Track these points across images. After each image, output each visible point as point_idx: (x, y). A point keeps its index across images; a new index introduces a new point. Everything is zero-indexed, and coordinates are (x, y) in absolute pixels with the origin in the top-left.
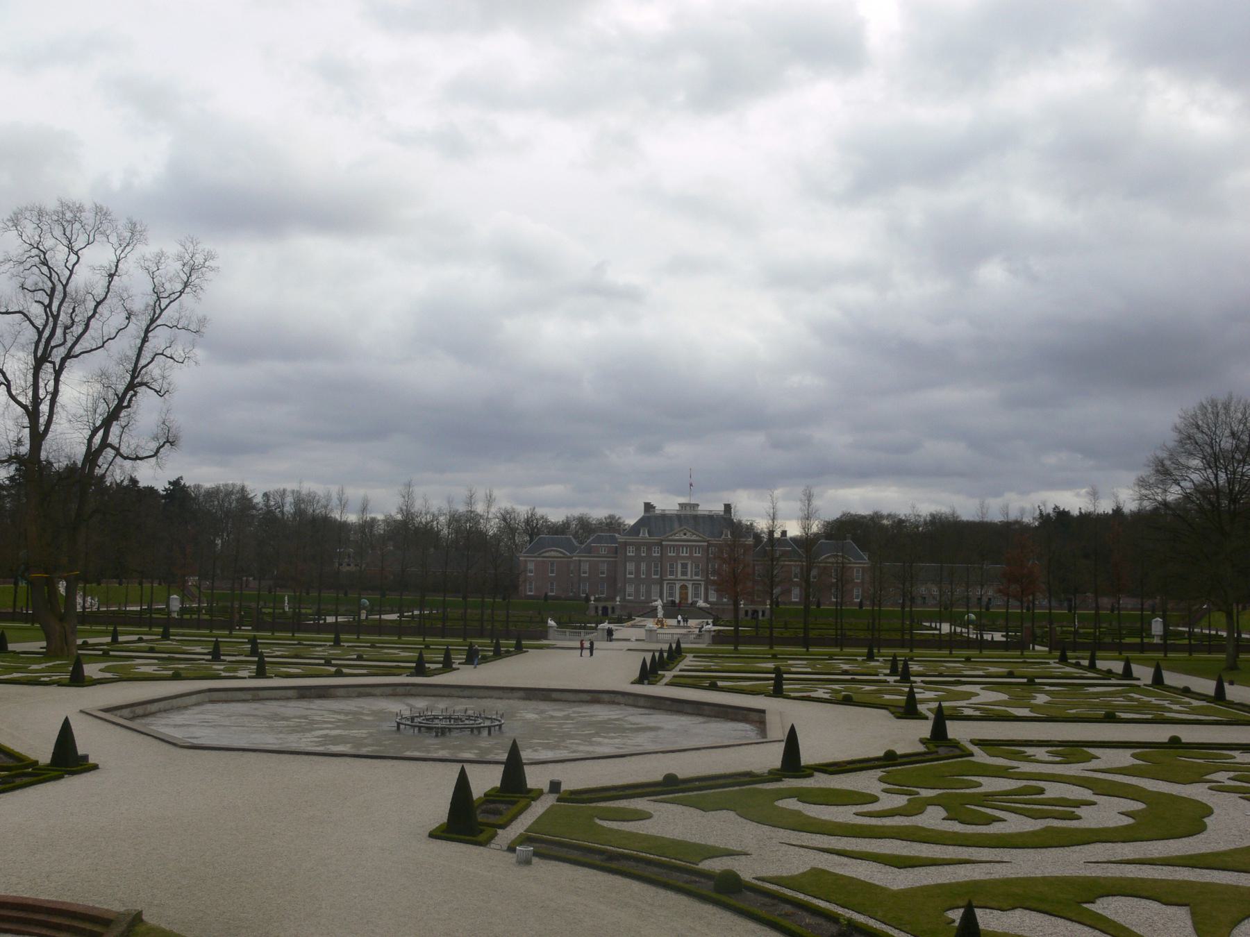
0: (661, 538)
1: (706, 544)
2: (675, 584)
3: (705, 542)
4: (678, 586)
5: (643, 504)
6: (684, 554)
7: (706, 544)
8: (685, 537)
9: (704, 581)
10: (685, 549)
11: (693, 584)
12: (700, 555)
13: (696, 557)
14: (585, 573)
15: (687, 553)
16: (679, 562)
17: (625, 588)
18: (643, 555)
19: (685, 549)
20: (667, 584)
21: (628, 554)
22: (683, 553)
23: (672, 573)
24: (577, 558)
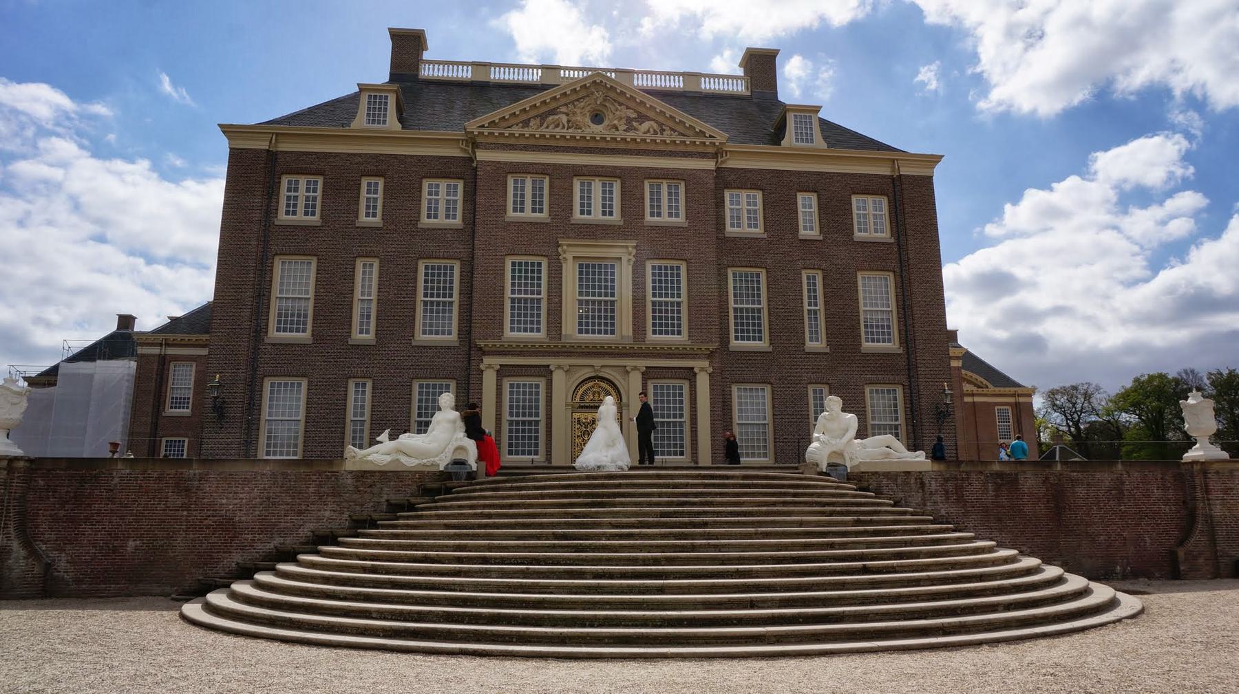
0: (472, 126)
1: (710, 165)
2: (546, 372)
3: (703, 155)
5: (387, 45)
6: (597, 216)
7: (710, 165)
8: (597, 130)
9: (710, 355)
11: (648, 374)
12: (681, 220)
13: (654, 228)
14: (177, 403)
17: (253, 405)
18: (363, 219)
20: (503, 372)
21: (283, 217)
22: (586, 209)
23: (525, 316)
24: (156, 351)
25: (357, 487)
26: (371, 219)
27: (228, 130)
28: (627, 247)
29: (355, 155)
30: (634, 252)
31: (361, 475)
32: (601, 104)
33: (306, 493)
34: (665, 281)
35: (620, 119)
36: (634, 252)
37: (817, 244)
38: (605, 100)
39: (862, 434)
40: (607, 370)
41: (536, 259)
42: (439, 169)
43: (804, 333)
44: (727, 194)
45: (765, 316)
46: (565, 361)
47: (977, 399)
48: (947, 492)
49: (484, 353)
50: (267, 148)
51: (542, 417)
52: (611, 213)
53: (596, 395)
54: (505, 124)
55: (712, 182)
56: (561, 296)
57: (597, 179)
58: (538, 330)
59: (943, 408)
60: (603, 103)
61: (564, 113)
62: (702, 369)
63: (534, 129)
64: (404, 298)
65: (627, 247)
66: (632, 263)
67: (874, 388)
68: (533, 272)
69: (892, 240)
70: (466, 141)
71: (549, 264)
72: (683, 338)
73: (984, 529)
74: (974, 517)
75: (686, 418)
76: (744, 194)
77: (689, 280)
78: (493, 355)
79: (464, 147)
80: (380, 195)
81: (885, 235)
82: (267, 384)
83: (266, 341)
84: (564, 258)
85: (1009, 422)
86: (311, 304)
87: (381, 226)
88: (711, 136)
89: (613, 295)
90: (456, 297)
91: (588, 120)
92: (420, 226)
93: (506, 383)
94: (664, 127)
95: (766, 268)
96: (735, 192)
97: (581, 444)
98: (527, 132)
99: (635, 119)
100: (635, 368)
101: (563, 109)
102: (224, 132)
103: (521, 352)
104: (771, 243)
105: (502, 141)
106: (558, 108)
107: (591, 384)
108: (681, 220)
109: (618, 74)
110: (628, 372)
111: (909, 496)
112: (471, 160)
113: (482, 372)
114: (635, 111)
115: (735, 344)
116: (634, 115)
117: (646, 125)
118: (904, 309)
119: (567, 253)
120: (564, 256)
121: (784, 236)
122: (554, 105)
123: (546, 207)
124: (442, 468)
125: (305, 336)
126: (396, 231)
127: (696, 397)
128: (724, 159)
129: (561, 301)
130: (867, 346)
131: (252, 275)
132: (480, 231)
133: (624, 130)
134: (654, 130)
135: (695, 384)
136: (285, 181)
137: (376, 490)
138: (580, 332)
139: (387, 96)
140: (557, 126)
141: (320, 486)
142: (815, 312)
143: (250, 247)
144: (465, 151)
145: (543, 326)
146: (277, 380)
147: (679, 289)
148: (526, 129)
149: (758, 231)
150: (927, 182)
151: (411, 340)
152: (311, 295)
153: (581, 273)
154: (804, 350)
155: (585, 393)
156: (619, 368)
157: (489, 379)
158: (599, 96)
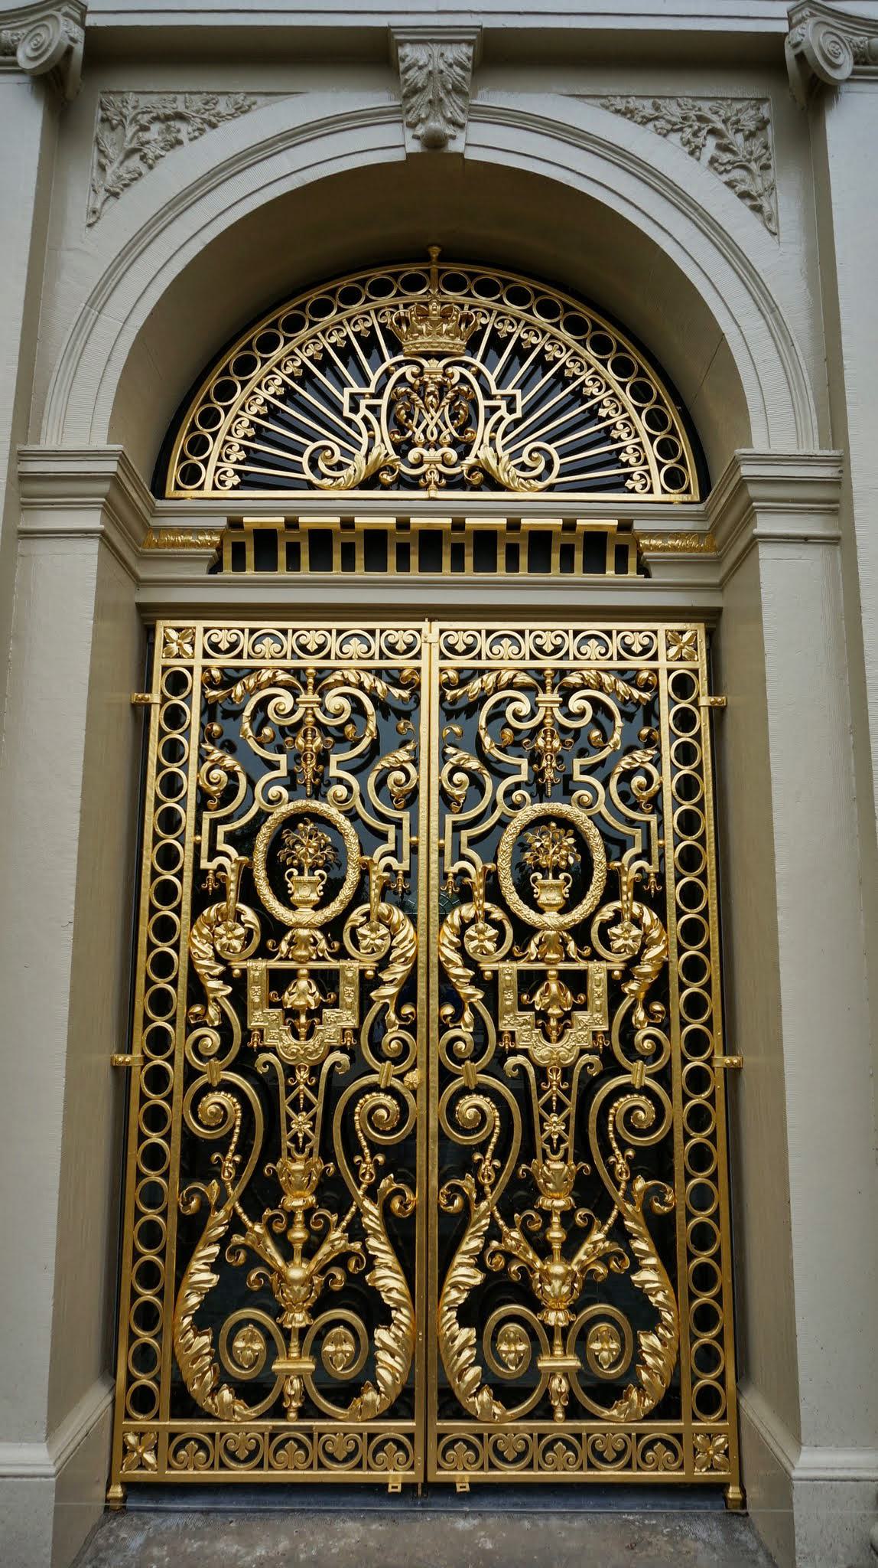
53: (433, 420)
97: (239, 985)
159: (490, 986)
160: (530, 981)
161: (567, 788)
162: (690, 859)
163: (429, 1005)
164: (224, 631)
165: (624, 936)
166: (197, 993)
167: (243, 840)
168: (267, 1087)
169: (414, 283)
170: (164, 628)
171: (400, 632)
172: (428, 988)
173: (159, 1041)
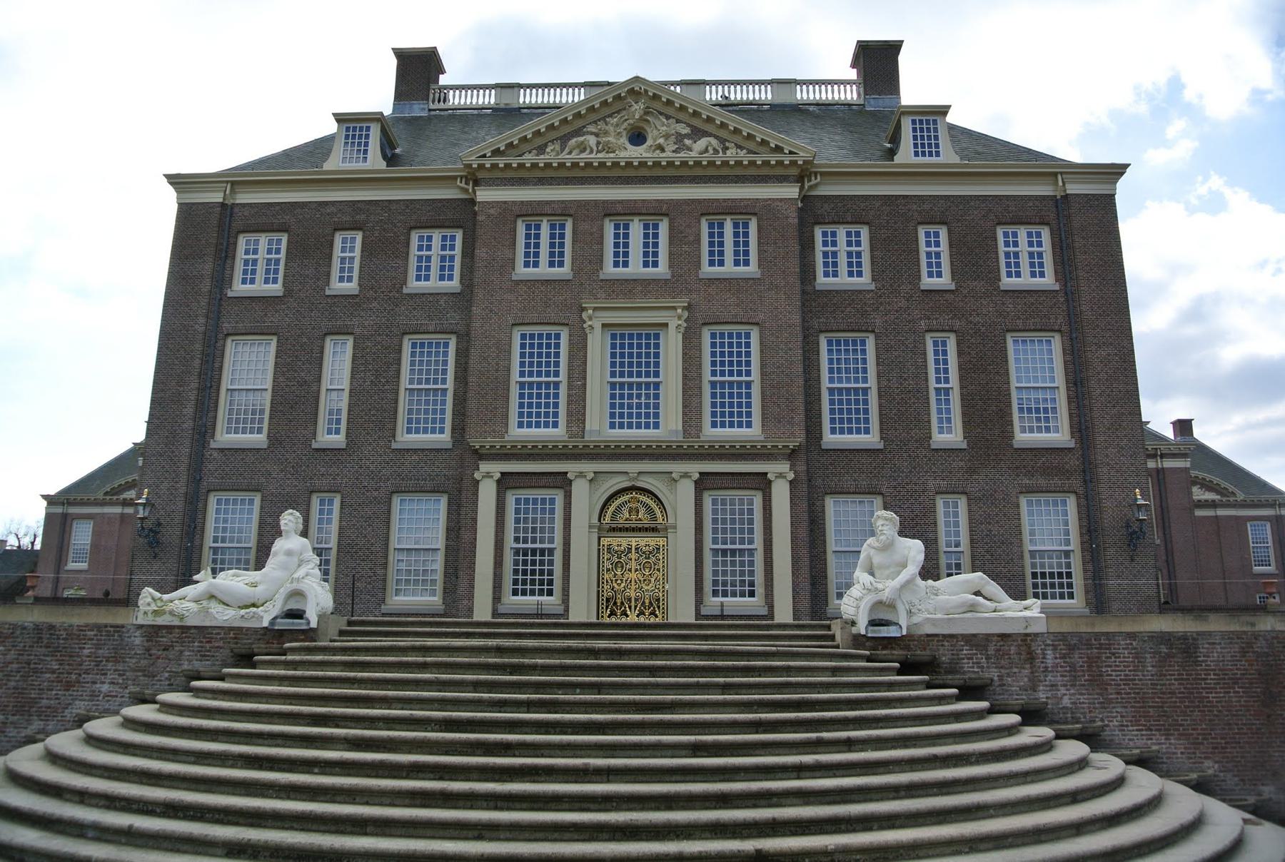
1: (791, 192)
2: (562, 482)
3: (782, 179)
4: (584, 500)
6: (636, 268)
9: (792, 455)
10: (636, 230)
11: (704, 483)
12: (752, 269)
13: (712, 281)
15: (650, 258)
16: (595, 323)
18: (338, 286)
19: (636, 230)
20: (506, 482)
21: (239, 288)
22: (622, 258)
25: (148, 650)
26: (345, 285)
27: (176, 181)
28: (674, 308)
29: (326, 203)
30: (686, 314)
31: (153, 632)
32: (641, 119)
33: (78, 656)
34: (732, 359)
35: (667, 136)
36: (686, 314)
37: (950, 297)
38: (647, 113)
39: (930, 571)
40: (650, 480)
41: (553, 330)
42: (432, 216)
43: (929, 422)
44: (818, 232)
45: (873, 398)
46: (589, 467)
47: (1221, 512)
48: (1073, 667)
49: (480, 455)
50: (221, 200)
51: (558, 544)
52: (655, 264)
54: (515, 152)
55: (795, 214)
56: (585, 378)
57: (636, 219)
58: (555, 425)
59: (1135, 527)
60: (646, 117)
61: (592, 133)
62: (781, 476)
63: (552, 155)
64: (384, 385)
65: (674, 308)
66: (682, 330)
67: (1034, 498)
68: (548, 346)
69: (1057, 287)
70: (466, 177)
71: (570, 336)
72: (753, 432)
73: (1137, 730)
74: (1119, 710)
75: (758, 544)
76: (841, 232)
77: (762, 351)
78: (493, 459)
79: (463, 185)
80: (357, 253)
81: (1048, 281)
82: (212, 500)
83: (213, 445)
84: (590, 326)
85: (1267, 543)
86: (268, 397)
87: (357, 293)
88: (791, 152)
89: (657, 374)
90: (450, 385)
91: (624, 140)
92: (405, 291)
93: (511, 499)
94: (727, 144)
95: (873, 331)
96: (829, 229)
97: (612, 581)
98: (542, 160)
99: (687, 136)
100: (686, 475)
101: (592, 128)
102: (171, 183)
103: (530, 455)
104: (881, 296)
105: (510, 174)
106: (584, 127)
107: (626, 498)
108: (752, 269)
109: (684, 86)
110: (676, 481)
111: (1008, 675)
112: (472, 202)
113: (478, 482)
114: (689, 125)
115: (831, 439)
116: (687, 131)
117: (702, 143)
118: (1075, 384)
119: (594, 319)
120: (590, 323)
121: (899, 286)
122: (580, 123)
123: (567, 259)
124: (265, 624)
125: (259, 439)
126: (375, 299)
127: (771, 515)
128: (812, 183)
129: (584, 385)
130: (1023, 437)
131: (197, 362)
132: (479, 294)
133: (673, 151)
134: (714, 149)
135: (770, 493)
136: (242, 241)
137: (171, 654)
138: (612, 426)
139: (369, 127)
140: (583, 150)
141: (98, 647)
142: (947, 391)
143: (197, 326)
144: (466, 191)
145: (562, 419)
146: (224, 496)
147: (748, 363)
148: (542, 157)
149: (865, 281)
150: (1107, 203)
151: (390, 441)
152: (268, 385)
153: (613, 346)
154: (929, 445)
155: (619, 509)
156: (663, 475)
157: (487, 494)
158: (638, 108)
159: (640, 581)
160: (645, 580)
161: (649, 558)
162: (663, 566)
163: (633, 583)
164: (609, 539)
165: (656, 575)
166: (607, 581)
167: (612, 564)
168: (615, 592)
169: (631, 493)
170: (602, 539)
171: (630, 539)
172: (633, 581)
173: (603, 587)
